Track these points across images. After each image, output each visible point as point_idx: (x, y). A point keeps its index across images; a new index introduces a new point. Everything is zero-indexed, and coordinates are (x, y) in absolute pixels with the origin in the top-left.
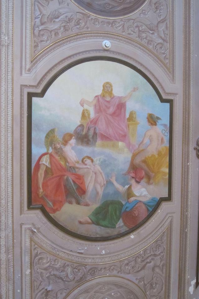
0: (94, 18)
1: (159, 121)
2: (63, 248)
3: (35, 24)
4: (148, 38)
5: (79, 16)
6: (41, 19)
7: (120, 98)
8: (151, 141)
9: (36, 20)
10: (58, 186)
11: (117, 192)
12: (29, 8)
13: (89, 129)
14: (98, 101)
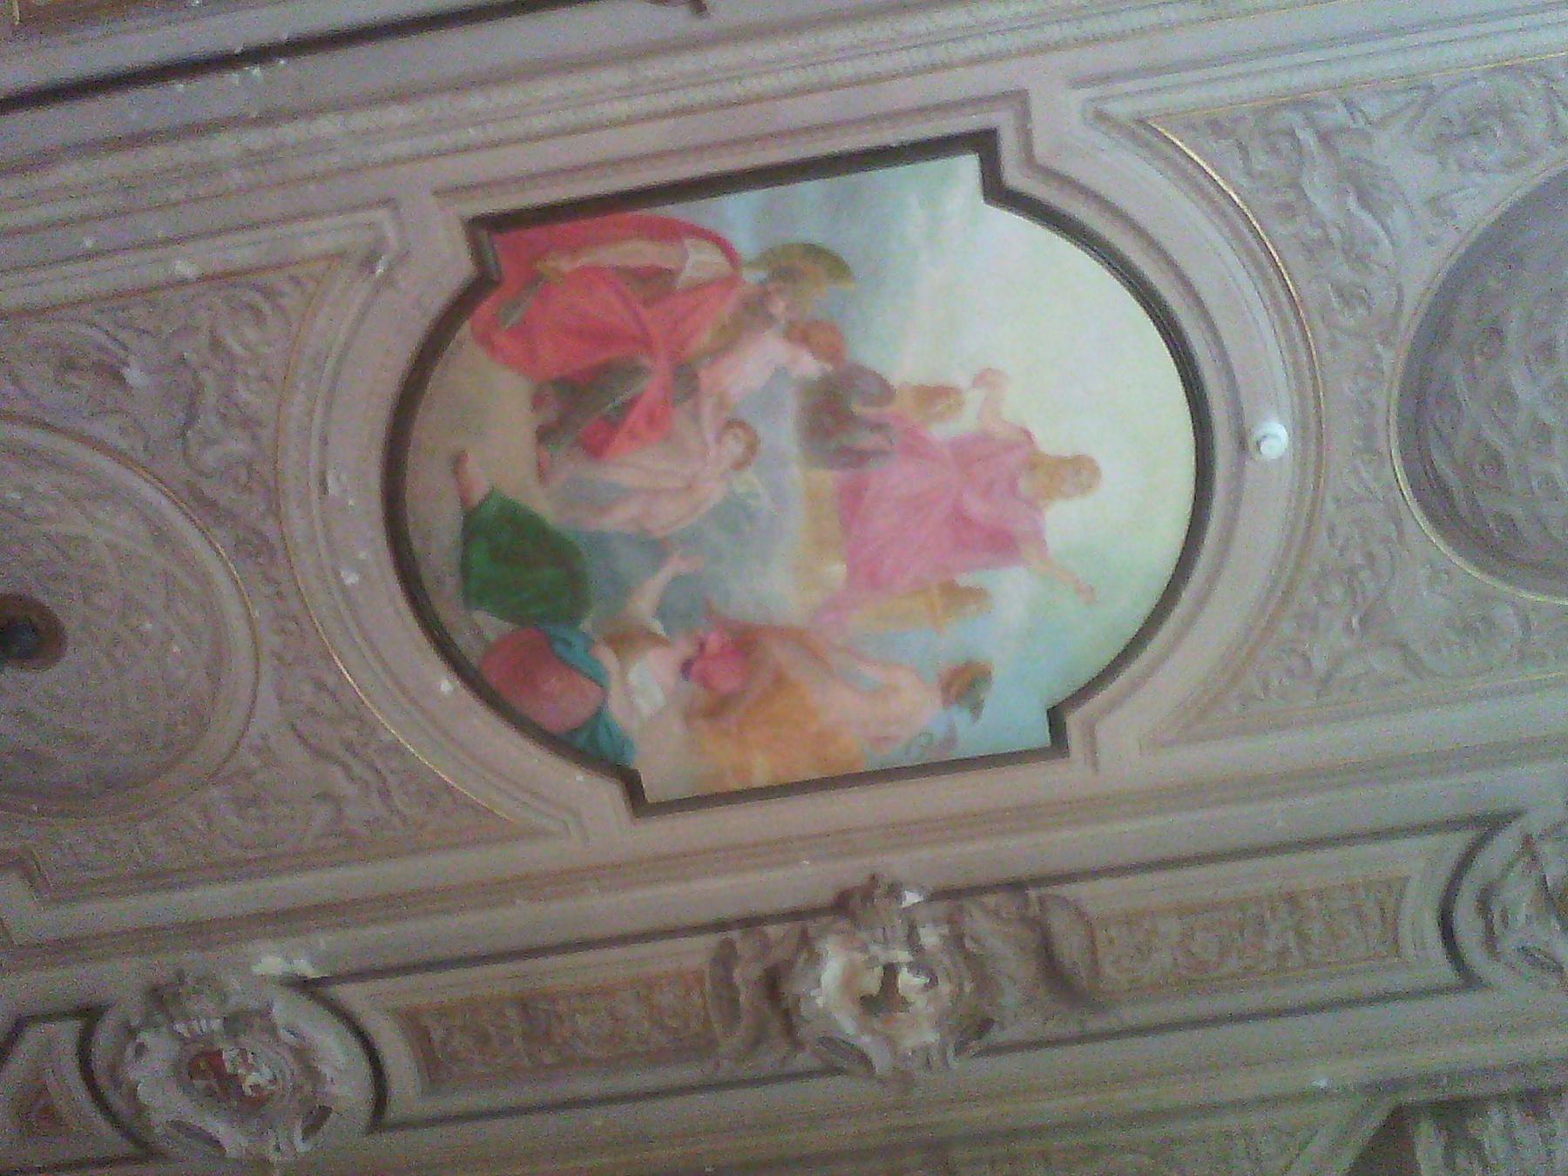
0: (1386, 367)
2: (329, 405)
3: (1318, 105)
4: (1324, 613)
6: (1349, 129)
7: (1037, 536)
9: (1340, 107)
10: (603, 336)
12: (1393, 64)
13: (878, 427)
14: (1010, 447)
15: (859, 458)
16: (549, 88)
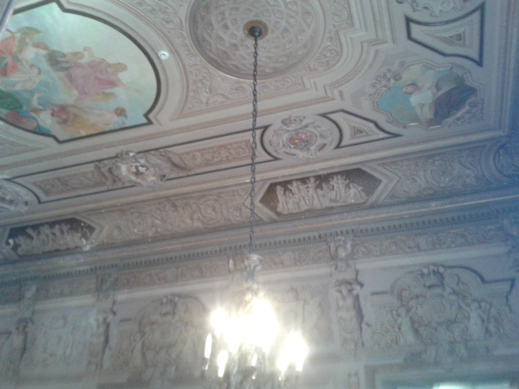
1: (124, 118)
7: (119, 80)
13: (67, 62)
15: (66, 69)
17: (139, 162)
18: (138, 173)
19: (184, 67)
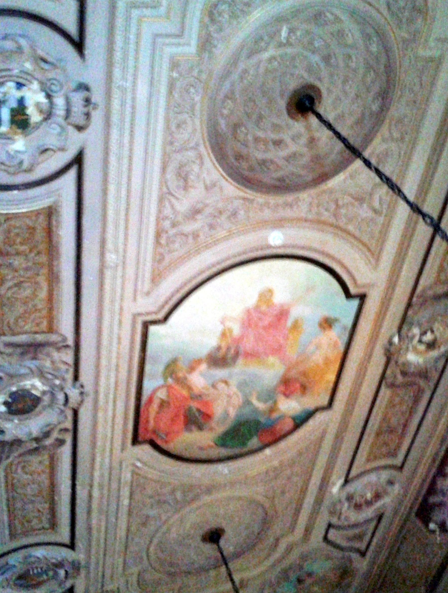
5: (237, 203)
8: (318, 347)
11: (256, 410)
13: (228, 349)
15: (237, 354)
16: (100, 428)
17: (414, 337)
18: (431, 345)
19: (306, 220)
